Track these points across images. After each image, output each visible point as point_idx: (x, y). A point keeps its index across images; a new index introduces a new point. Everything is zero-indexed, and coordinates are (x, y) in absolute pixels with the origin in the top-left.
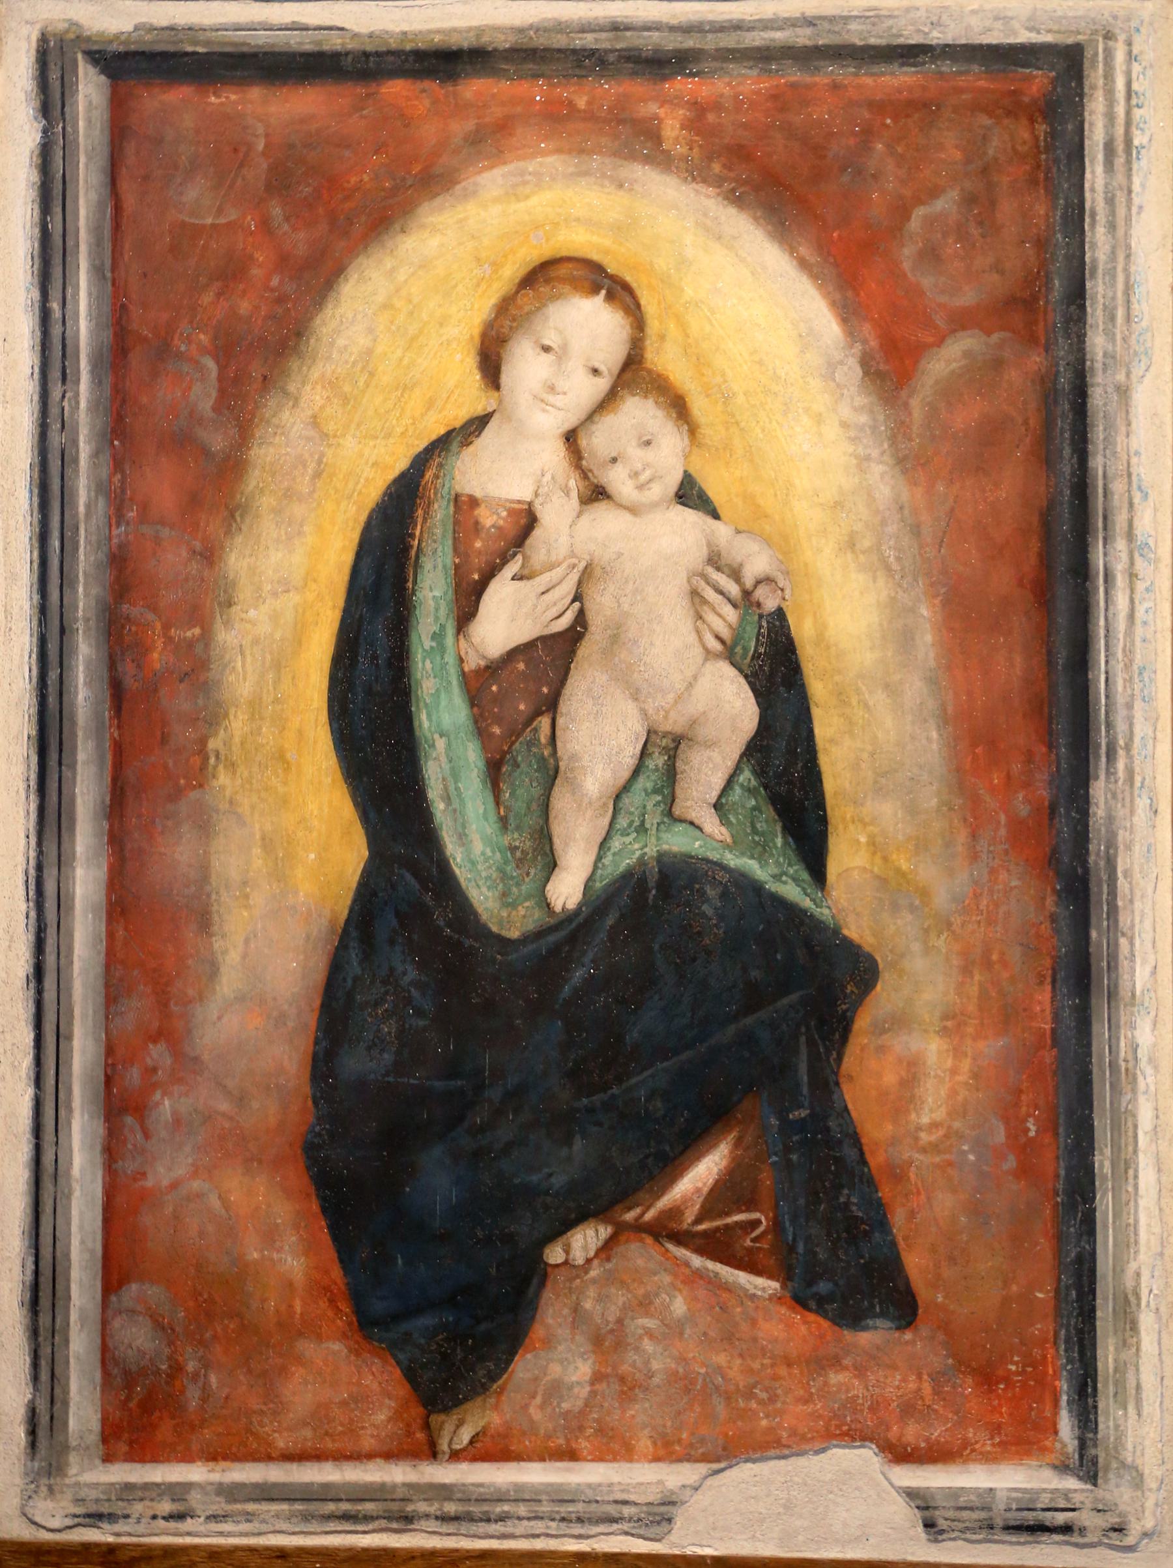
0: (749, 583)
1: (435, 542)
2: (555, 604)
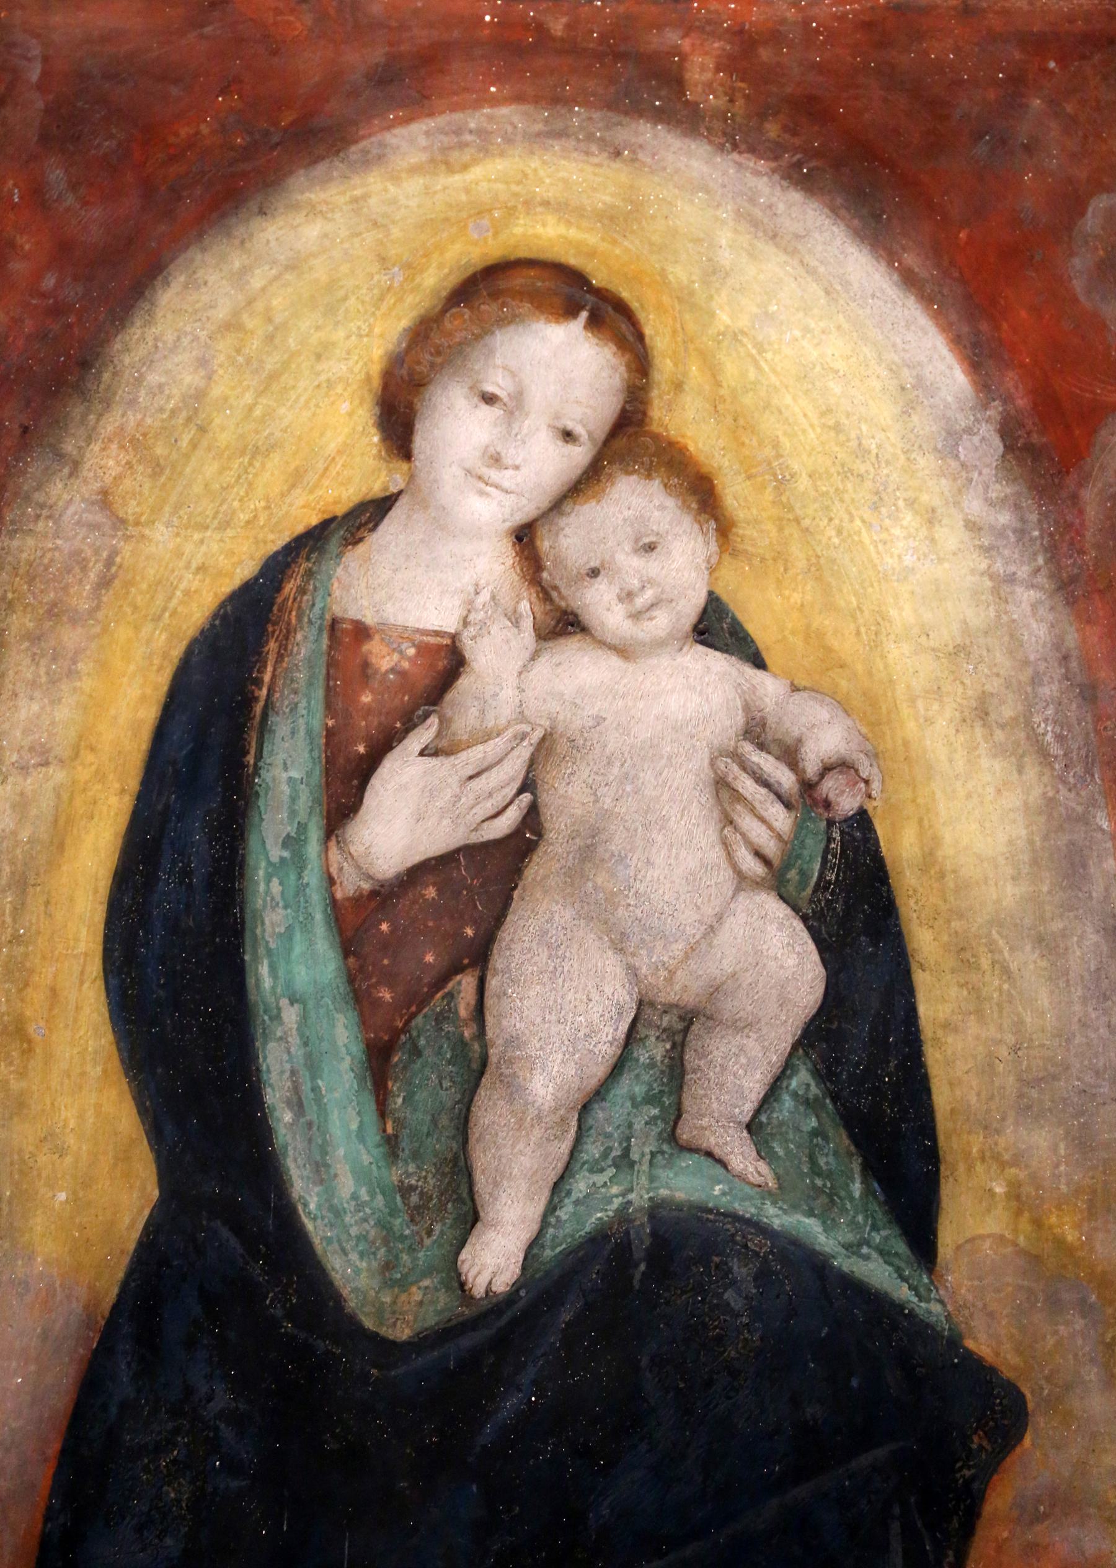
0: (811, 768)
1: (296, 693)
2: (490, 795)
